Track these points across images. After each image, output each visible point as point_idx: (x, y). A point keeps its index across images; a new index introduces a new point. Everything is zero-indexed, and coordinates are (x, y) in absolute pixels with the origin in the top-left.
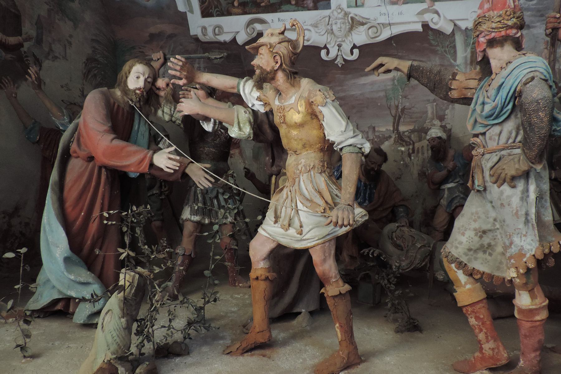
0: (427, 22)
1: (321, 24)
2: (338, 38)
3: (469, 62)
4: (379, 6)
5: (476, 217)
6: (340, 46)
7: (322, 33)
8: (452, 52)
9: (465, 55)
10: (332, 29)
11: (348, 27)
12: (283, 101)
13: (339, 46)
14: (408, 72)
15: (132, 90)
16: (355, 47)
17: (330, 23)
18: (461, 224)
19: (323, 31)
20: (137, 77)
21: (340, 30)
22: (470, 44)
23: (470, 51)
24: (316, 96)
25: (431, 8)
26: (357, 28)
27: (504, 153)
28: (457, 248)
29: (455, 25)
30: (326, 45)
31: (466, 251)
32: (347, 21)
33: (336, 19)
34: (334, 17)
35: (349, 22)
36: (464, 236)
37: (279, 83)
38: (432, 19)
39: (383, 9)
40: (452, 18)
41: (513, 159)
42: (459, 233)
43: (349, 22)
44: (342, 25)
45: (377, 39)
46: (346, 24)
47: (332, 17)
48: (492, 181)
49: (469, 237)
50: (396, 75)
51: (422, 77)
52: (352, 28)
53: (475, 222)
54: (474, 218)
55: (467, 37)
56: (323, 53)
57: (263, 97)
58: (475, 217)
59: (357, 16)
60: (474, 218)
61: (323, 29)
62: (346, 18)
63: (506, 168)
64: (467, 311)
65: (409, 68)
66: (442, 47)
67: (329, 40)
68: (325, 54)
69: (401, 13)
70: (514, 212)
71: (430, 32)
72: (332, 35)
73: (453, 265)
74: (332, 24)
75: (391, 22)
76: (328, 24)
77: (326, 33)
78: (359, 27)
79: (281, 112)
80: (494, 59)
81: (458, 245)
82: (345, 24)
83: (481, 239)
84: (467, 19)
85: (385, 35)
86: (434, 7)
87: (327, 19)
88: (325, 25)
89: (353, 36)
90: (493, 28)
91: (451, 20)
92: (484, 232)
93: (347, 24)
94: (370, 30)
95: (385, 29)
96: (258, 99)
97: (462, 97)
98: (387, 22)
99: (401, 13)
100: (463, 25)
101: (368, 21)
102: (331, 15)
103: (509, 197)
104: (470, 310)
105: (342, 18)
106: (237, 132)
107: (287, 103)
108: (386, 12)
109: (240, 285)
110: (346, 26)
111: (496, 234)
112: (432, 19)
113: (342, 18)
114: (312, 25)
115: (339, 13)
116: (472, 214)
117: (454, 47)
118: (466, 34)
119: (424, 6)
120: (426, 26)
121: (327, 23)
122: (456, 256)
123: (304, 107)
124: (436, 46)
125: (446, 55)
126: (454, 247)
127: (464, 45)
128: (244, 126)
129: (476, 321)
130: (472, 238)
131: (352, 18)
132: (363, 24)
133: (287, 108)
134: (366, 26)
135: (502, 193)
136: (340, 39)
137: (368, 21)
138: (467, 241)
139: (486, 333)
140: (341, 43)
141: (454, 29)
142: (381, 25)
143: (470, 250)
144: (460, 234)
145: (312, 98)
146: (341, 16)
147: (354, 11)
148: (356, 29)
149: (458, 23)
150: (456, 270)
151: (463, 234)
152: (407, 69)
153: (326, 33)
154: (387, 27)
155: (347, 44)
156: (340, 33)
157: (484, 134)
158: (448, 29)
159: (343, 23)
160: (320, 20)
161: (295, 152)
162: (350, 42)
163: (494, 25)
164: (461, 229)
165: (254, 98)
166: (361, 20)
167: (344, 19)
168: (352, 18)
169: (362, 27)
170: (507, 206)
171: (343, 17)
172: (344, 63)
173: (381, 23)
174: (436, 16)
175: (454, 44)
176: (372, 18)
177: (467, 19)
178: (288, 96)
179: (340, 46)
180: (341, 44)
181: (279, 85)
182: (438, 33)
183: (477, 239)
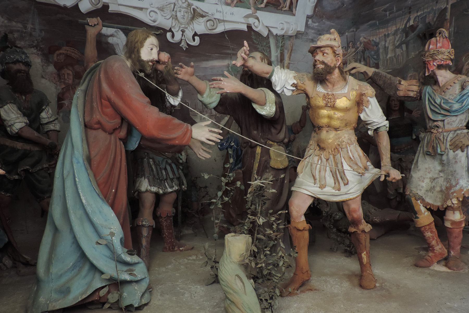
0: (251, 24)
1: (167, 9)
2: (181, 24)
3: (279, 60)
4: (217, 4)
5: (429, 171)
6: (183, 31)
7: (168, 17)
8: (268, 50)
9: (277, 54)
10: (176, 16)
11: (190, 16)
12: (330, 90)
13: (182, 32)
14: (372, 75)
15: (146, 61)
16: (195, 34)
17: (175, 9)
18: (420, 175)
19: (168, 15)
20: (151, 49)
21: (183, 17)
22: (279, 47)
23: (280, 53)
24: (367, 89)
25: (254, 14)
26: (198, 18)
27: (459, 132)
28: (421, 190)
29: (269, 31)
30: (171, 28)
31: (425, 191)
32: (189, 11)
33: (181, 7)
34: (179, 5)
35: (191, 13)
36: (424, 182)
37: (333, 77)
38: (254, 23)
39: (219, 7)
40: (267, 26)
41: (465, 136)
42: (420, 181)
43: (191, 13)
44: (185, 14)
45: (214, 31)
46: (188, 13)
47: (177, 5)
48: (450, 148)
49: (427, 182)
50: (230, 63)
51: (380, 80)
52: (194, 18)
53: (429, 173)
54: (428, 171)
55: (277, 41)
56: (169, 35)
57: (300, 84)
58: (428, 170)
59: (198, 8)
60: (428, 171)
61: (168, 14)
62: (189, 8)
63: (463, 141)
64: (425, 229)
65: (373, 73)
66: (262, 46)
67: (173, 25)
68: (170, 37)
69: (233, 14)
70: (462, 165)
71: (253, 33)
72: (177, 21)
73: (419, 201)
74: (176, 11)
75: (225, 19)
76: (173, 10)
77: (171, 18)
78: (199, 18)
79: (332, 98)
80: (441, 76)
81: (421, 189)
82: (187, 13)
83: (432, 183)
84: (277, 28)
85: (220, 29)
86: (256, 14)
87: (172, 6)
88: (170, 11)
89: (194, 25)
90: (444, 59)
91: (267, 27)
92: (434, 179)
93: (190, 14)
94: (208, 23)
95: (220, 24)
96: (293, 85)
97: (407, 95)
98: (222, 18)
99: (233, 14)
100: (275, 32)
101: (207, 14)
102: (176, 3)
103: (461, 157)
104: (427, 228)
105: (185, 8)
106: (268, 110)
107: (337, 93)
108: (222, 11)
109: (181, 249)
110: (188, 15)
111: (438, 180)
112: (254, 23)
113: (185, 8)
114: (158, 8)
115: (183, 3)
116: (426, 169)
117: (269, 47)
118: (277, 39)
119: (249, 12)
120: (249, 27)
121: (172, 9)
122: (421, 195)
123: (355, 97)
124: (257, 44)
125: (265, 53)
126: (418, 190)
127: (275, 47)
128: (271, 106)
129: (431, 234)
130: (428, 183)
131: (194, 10)
132: (203, 16)
133: (339, 96)
134: (205, 18)
135: (457, 155)
136: (183, 26)
137: (207, 14)
138: (426, 186)
139: (436, 240)
140: (184, 29)
141: (269, 34)
142: (217, 20)
143: (427, 191)
144: (421, 182)
145: (364, 91)
146: (184, 5)
147: (196, 4)
148: (197, 19)
149: (271, 29)
150: (420, 204)
151: (423, 181)
152: (372, 73)
153: (171, 18)
154: (221, 22)
155: (190, 32)
156: (183, 20)
157: (444, 121)
158: (265, 33)
159: (186, 12)
160: (166, 5)
161: (336, 129)
162: (192, 30)
163: (445, 57)
164: (421, 178)
165: (289, 84)
166: (201, 13)
167: (187, 9)
168: (194, 10)
169: (202, 18)
170: (459, 163)
171: (186, 7)
172: (187, 47)
173: (217, 19)
174: (256, 21)
175: (269, 45)
176: (210, 13)
177: (277, 28)
178: (336, 87)
179: (183, 31)
180: (185, 30)
181: (332, 78)
182: (258, 34)
183: (430, 183)
